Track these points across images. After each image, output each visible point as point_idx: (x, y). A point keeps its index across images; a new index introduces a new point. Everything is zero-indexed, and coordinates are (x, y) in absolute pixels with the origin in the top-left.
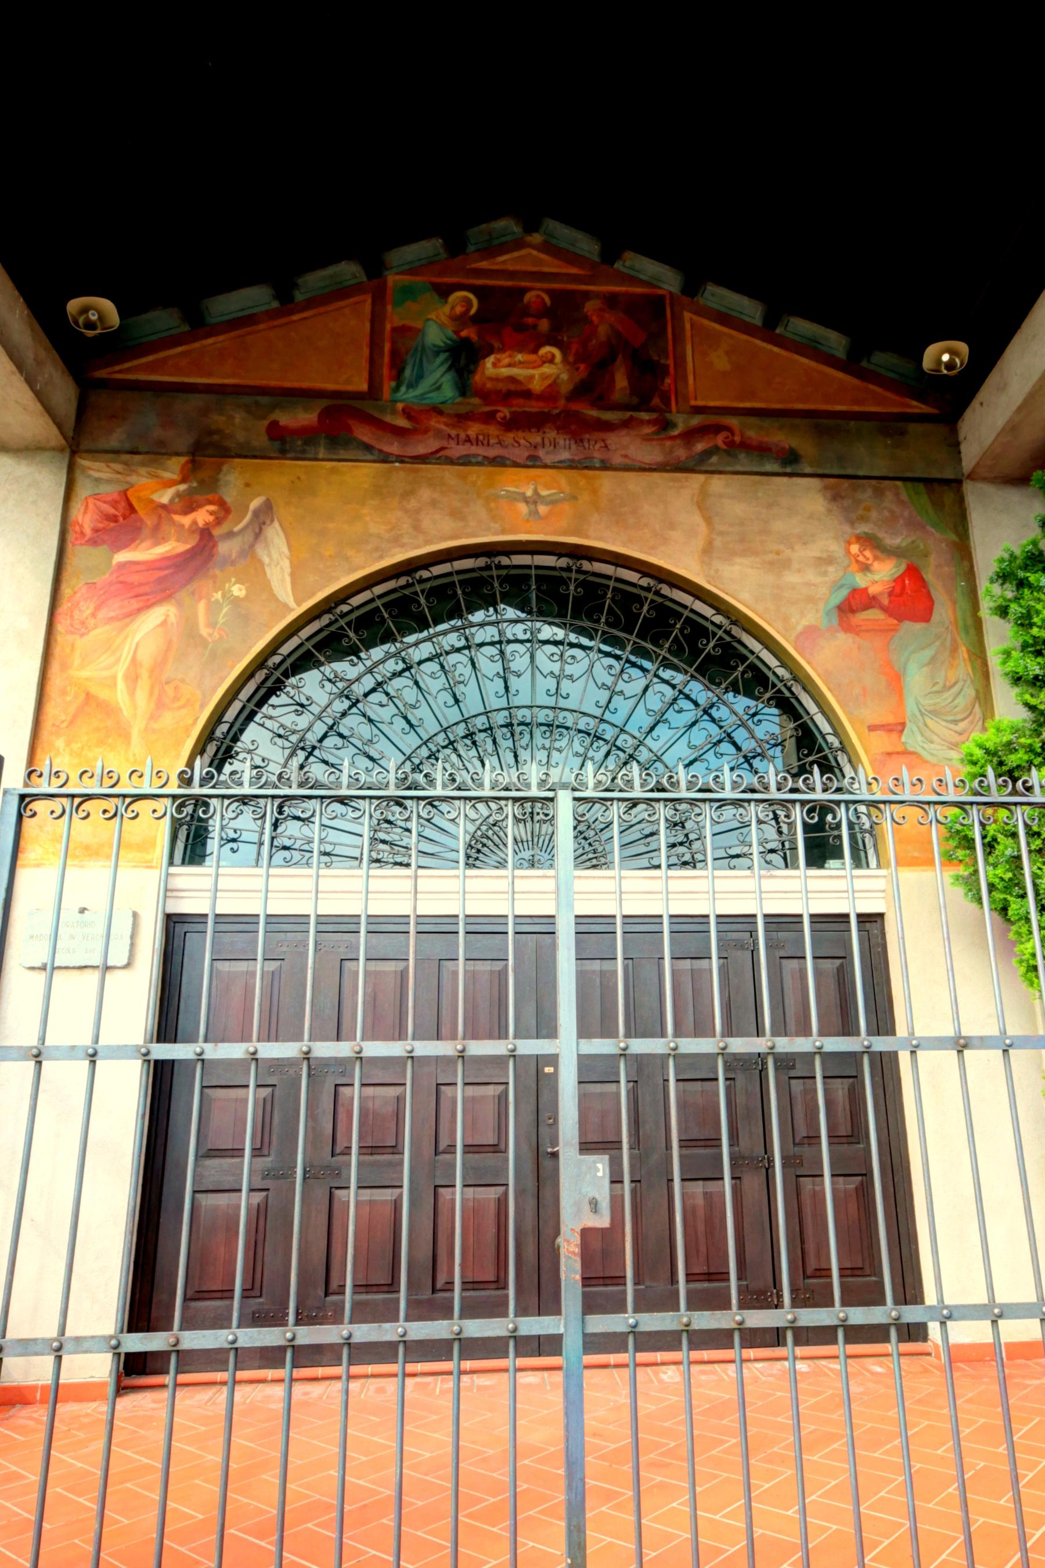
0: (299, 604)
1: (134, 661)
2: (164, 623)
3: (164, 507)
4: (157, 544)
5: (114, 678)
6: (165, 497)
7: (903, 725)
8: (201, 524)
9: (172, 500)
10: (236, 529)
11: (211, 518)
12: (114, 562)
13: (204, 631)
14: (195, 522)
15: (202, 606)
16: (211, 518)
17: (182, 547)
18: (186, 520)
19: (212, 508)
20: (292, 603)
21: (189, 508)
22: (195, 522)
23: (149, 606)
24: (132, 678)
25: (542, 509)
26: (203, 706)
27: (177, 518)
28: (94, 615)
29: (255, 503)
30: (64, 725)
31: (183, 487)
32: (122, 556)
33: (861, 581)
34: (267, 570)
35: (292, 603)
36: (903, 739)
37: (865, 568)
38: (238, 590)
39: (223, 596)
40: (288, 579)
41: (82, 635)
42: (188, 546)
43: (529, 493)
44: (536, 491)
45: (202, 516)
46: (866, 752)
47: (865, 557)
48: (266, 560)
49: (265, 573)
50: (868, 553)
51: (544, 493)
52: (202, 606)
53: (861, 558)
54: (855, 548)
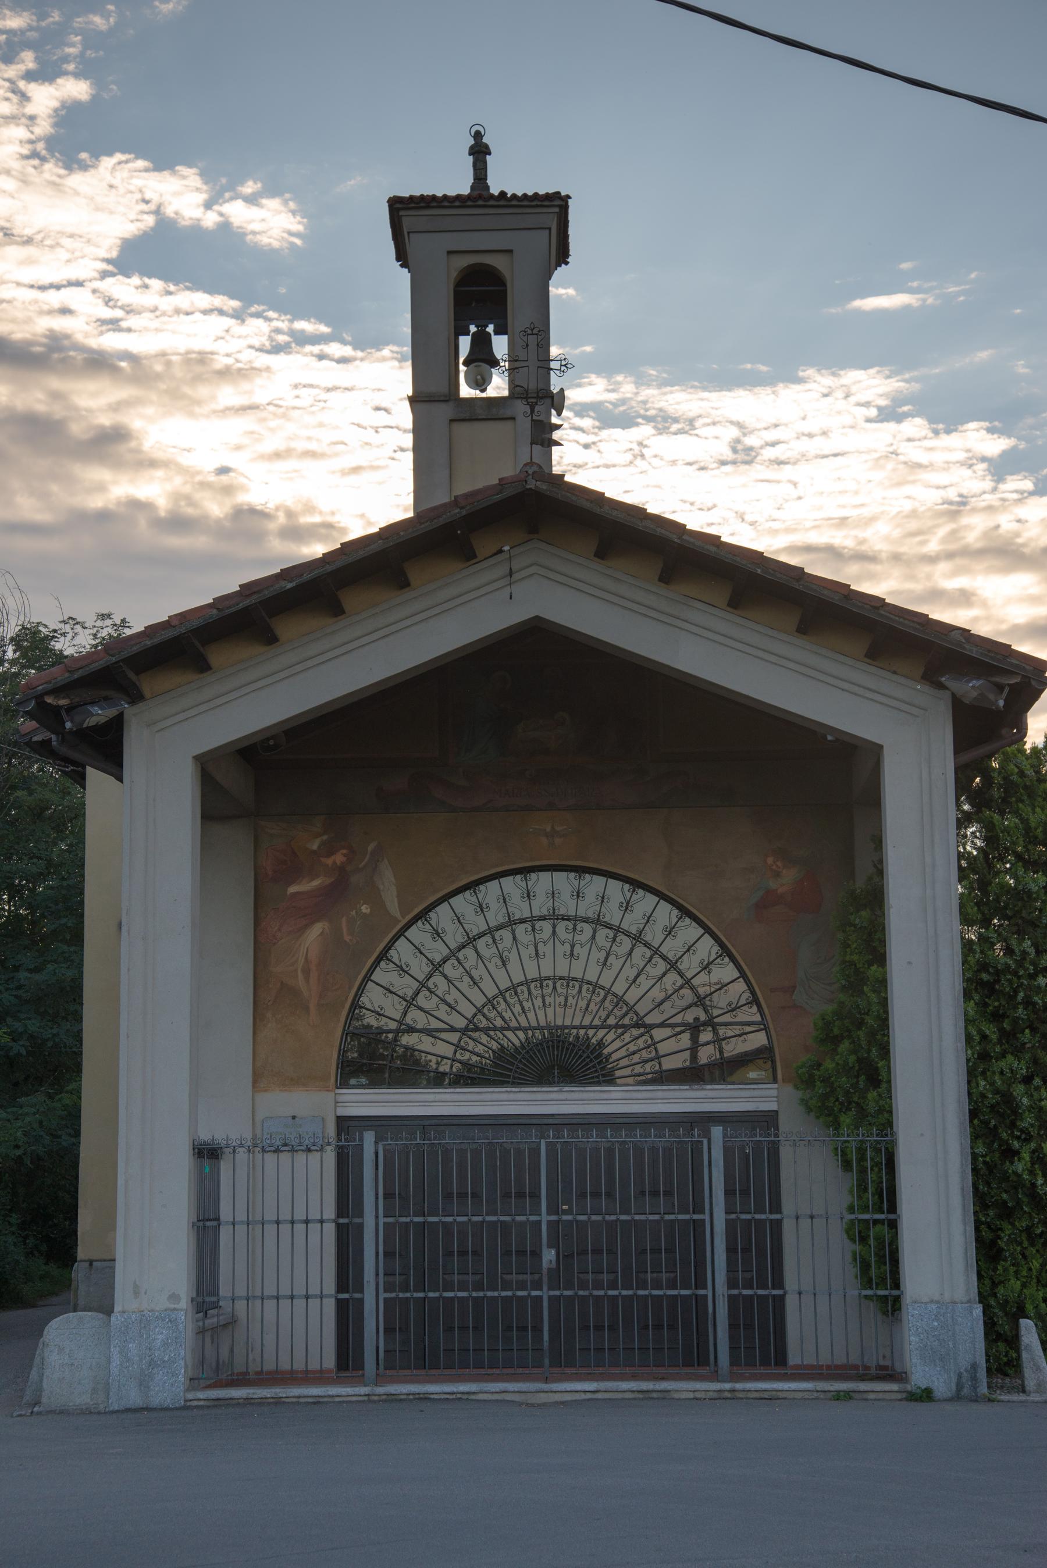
0: (404, 918)
1: (306, 958)
2: (322, 933)
3: (314, 852)
4: (313, 879)
5: (296, 970)
6: (315, 846)
7: (795, 987)
8: (338, 863)
9: (319, 847)
10: (361, 866)
11: (345, 859)
12: (288, 893)
13: (347, 938)
14: (335, 863)
15: (344, 920)
16: (345, 859)
17: (329, 881)
18: (329, 861)
19: (345, 851)
20: (398, 915)
21: (330, 853)
22: (335, 863)
23: (313, 922)
24: (307, 972)
25: (558, 841)
26: (350, 988)
27: (323, 859)
28: (279, 930)
29: (370, 848)
30: (271, 1002)
31: (325, 837)
32: (293, 889)
33: (772, 884)
34: (382, 894)
35: (398, 915)
36: (793, 997)
37: (777, 875)
38: (365, 909)
39: (356, 912)
40: (396, 900)
41: (275, 944)
42: (333, 880)
43: (549, 829)
44: (553, 828)
45: (339, 858)
46: (768, 1007)
47: (777, 866)
48: (381, 887)
49: (381, 896)
50: (779, 863)
51: (558, 828)
52: (344, 920)
53: (774, 867)
54: (770, 860)
